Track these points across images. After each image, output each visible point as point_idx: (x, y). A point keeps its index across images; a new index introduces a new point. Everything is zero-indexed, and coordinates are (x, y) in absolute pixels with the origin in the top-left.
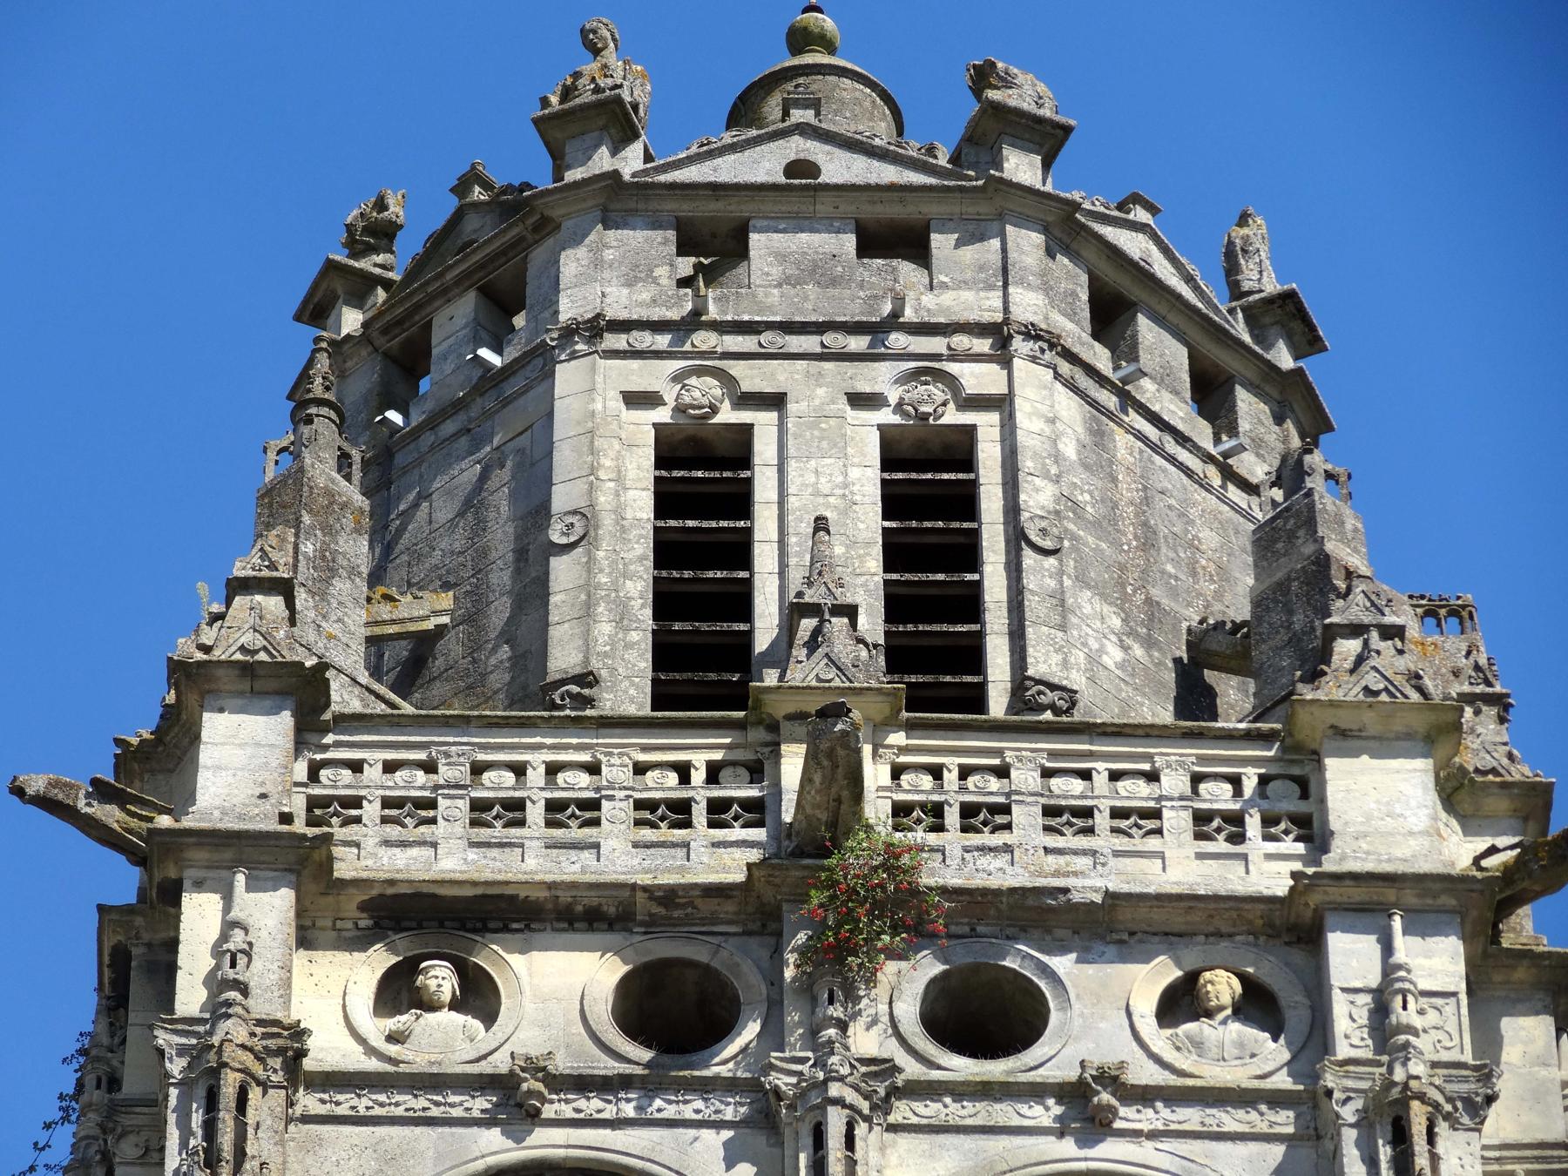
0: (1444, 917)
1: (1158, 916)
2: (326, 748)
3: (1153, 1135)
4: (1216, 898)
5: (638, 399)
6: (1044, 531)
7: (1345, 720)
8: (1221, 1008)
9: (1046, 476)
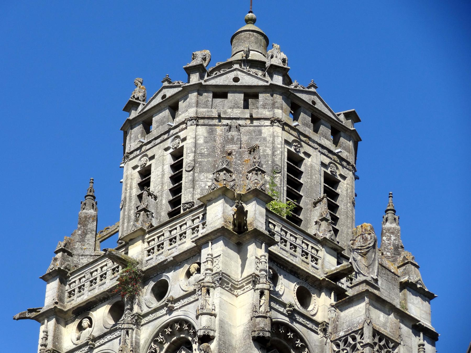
0: (218, 238)
1: (182, 257)
2: (70, 280)
3: (180, 308)
4: (188, 250)
5: (134, 168)
6: (189, 167)
7: (208, 198)
8: (193, 273)
9: (192, 152)
